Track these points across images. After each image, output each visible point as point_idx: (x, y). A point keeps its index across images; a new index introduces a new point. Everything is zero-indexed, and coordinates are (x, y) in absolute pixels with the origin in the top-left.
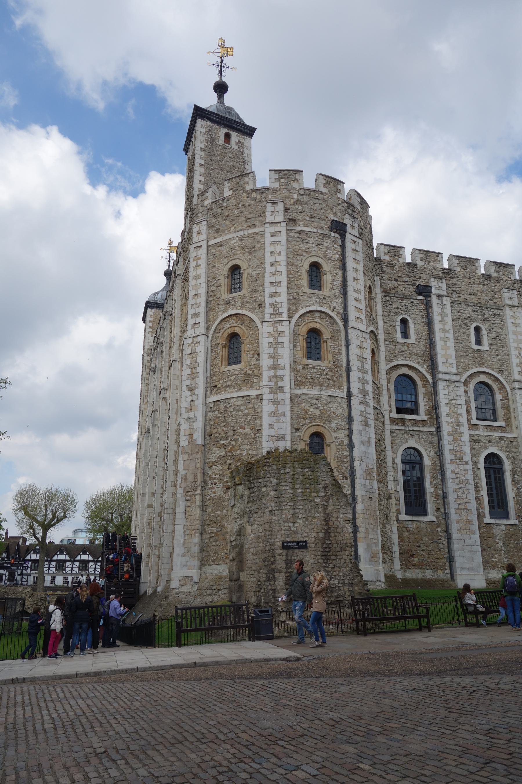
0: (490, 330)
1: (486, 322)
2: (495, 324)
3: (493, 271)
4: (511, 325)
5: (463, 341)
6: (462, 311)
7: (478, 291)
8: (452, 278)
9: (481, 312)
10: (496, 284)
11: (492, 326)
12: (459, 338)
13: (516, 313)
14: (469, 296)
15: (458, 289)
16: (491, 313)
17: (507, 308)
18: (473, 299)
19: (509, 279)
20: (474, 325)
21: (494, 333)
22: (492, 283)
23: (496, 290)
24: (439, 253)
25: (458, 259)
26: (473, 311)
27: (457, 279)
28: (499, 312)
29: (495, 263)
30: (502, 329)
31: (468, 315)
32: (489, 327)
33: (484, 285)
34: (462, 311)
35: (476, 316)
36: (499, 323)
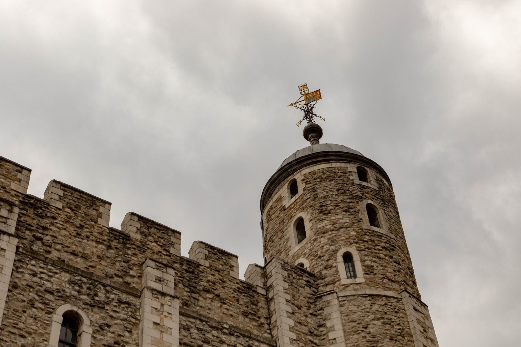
0: (101, 328)
1: (95, 310)
2: (118, 318)
3: (135, 230)
4: (151, 325)
5: (30, 333)
6: (43, 276)
7: (93, 253)
8: (42, 217)
9: (89, 288)
10: (136, 252)
11: (109, 321)
12: (21, 325)
13: (165, 306)
14: (72, 257)
15: (48, 238)
16: (112, 296)
17: (147, 293)
18: (80, 264)
19: (164, 252)
20: (67, 307)
21: (109, 334)
22: (129, 248)
23: (132, 262)
24: (23, 168)
25: (64, 191)
26: (70, 282)
27: (51, 220)
28: (131, 299)
29: (141, 218)
30: (130, 332)
31: (55, 287)
32: (101, 322)
33: (109, 247)
34: (43, 276)
35: (74, 293)
36: (125, 320)
